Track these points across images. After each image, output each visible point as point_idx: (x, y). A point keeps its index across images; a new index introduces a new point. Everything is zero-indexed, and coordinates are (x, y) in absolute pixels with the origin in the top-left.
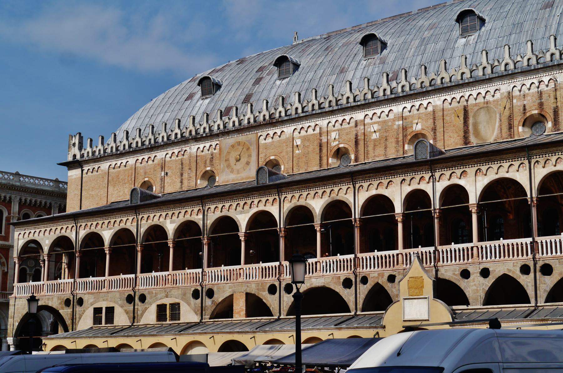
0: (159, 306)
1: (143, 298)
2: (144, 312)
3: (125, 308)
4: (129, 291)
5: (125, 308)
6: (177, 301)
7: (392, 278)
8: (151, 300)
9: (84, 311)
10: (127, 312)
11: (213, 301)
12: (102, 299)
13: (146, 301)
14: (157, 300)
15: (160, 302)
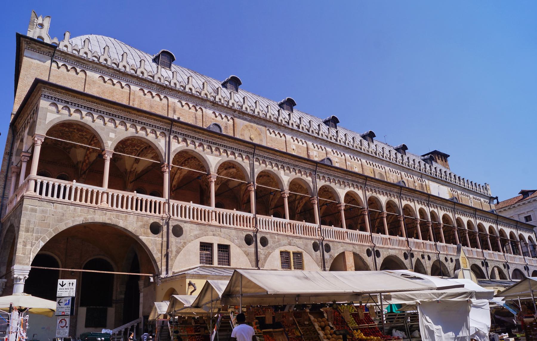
0: (281, 253)
1: (264, 242)
2: (267, 256)
3: (244, 249)
4: (250, 229)
5: (244, 249)
6: (300, 250)
7: (423, 257)
8: (274, 245)
9: (185, 243)
10: (247, 255)
11: (331, 255)
12: (212, 233)
13: (269, 245)
14: (280, 245)
15: (283, 249)
